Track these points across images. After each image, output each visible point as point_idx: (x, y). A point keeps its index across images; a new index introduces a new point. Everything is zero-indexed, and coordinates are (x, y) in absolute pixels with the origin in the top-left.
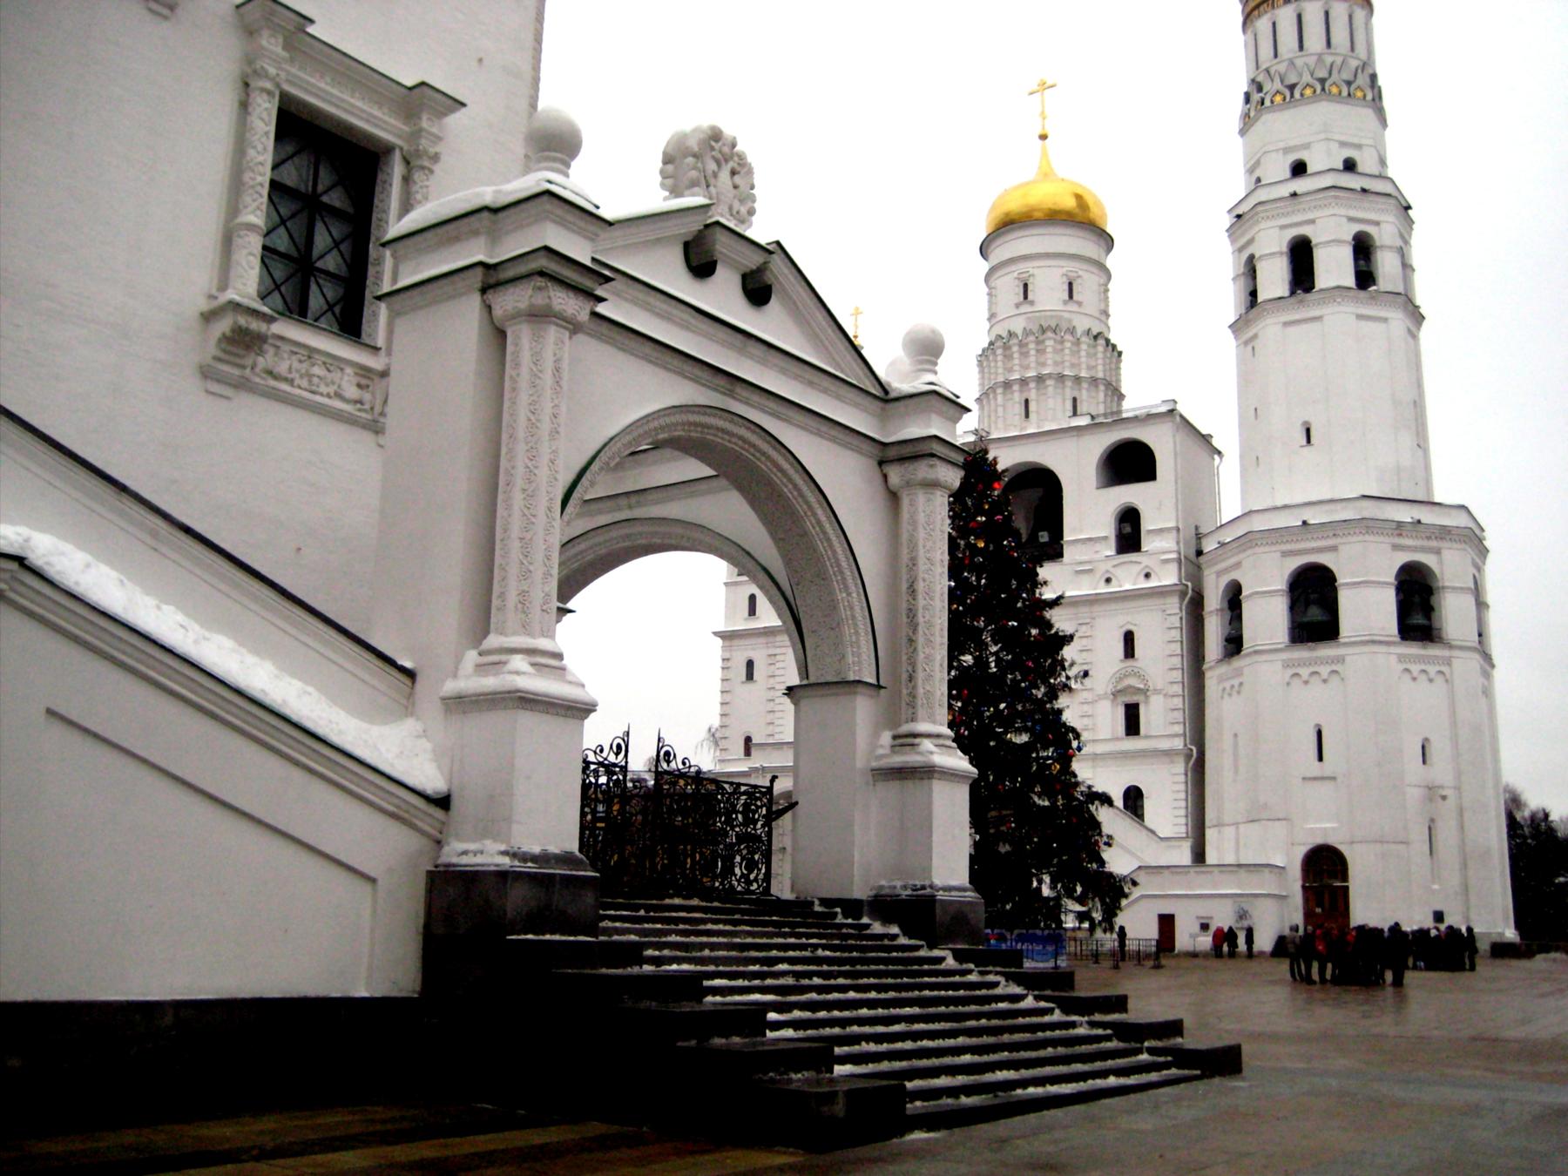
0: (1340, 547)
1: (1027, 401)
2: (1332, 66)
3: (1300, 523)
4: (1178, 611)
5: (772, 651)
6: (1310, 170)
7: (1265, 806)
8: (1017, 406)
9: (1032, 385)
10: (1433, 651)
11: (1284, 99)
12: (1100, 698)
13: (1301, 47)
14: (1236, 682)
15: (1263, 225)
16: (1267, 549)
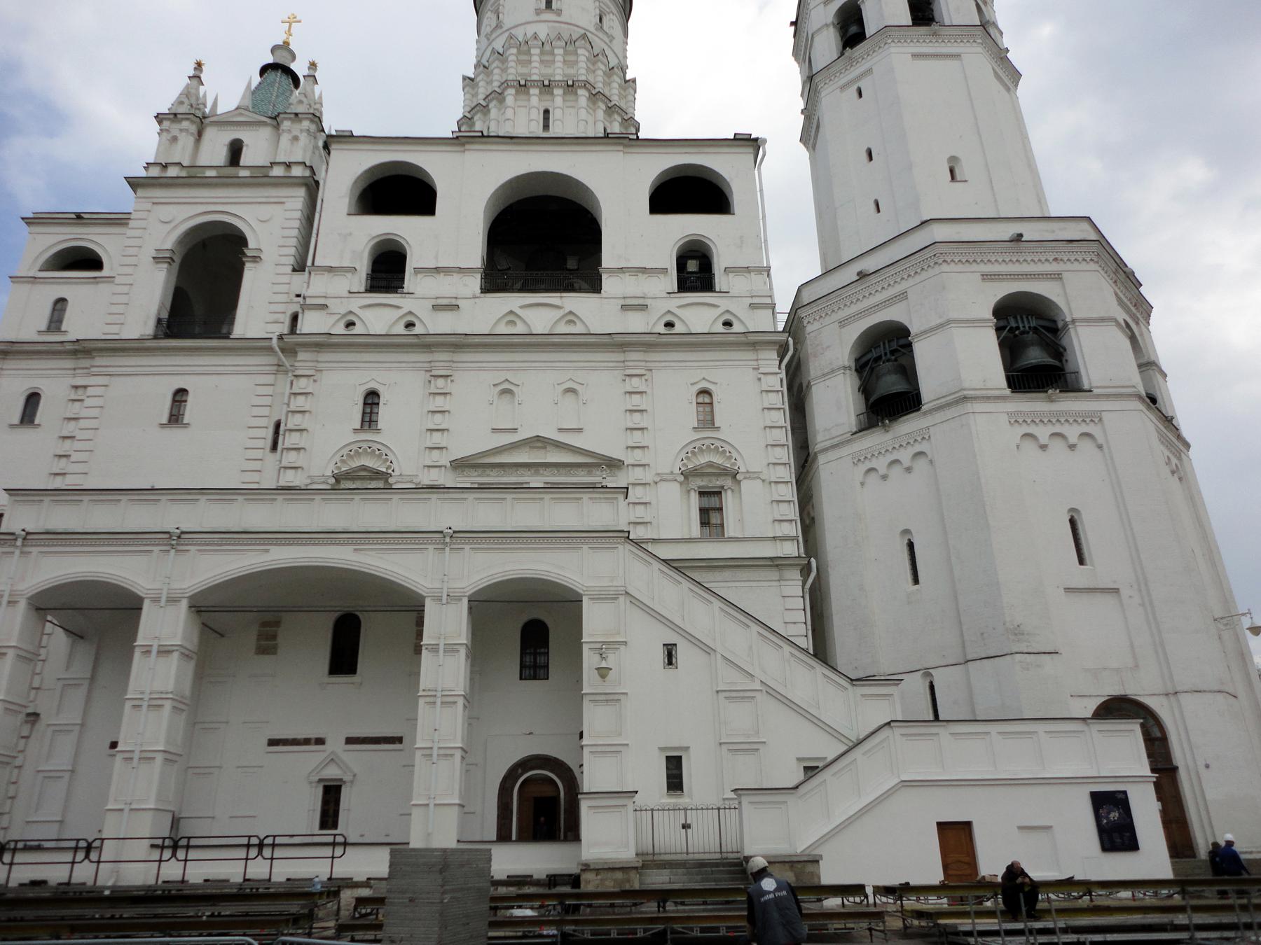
0: (1065, 275)
1: (546, 112)
4: (778, 371)
5: (80, 381)
7: (1018, 632)
8: (534, 112)
9: (558, 92)
12: (662, 479)
14: (905, 456)
16: (960, 267)
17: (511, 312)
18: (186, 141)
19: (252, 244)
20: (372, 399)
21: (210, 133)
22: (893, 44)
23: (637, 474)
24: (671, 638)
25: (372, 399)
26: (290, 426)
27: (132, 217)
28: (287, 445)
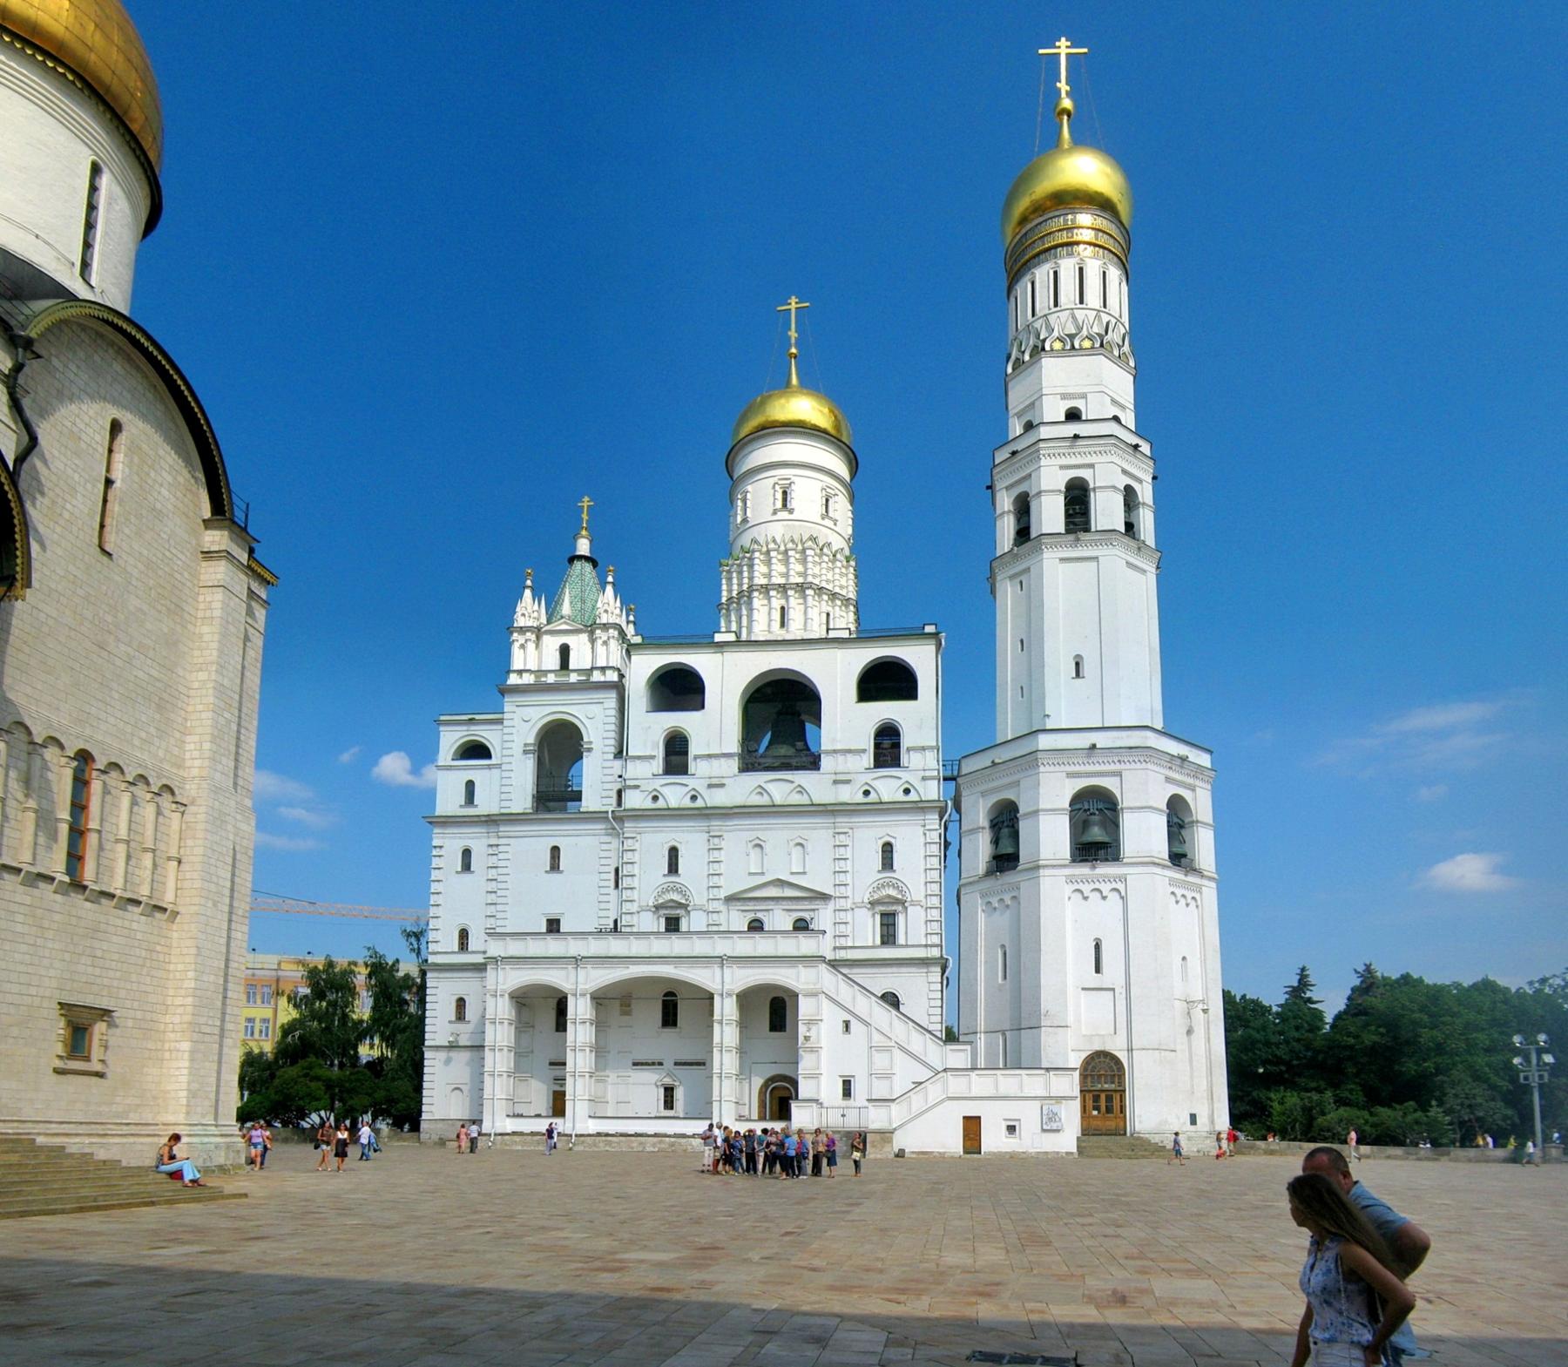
2: (1108, 324)
6: (1084, 418)
10: (1191, 879)
11: (1063, 349)
13: (1081, 302)
17: (760, 786)
18: (531, 646)
19: (585, 739)
20: (673, 853)
21: (546, 639)
23: (842, 903)
24: (848, 1017)
25: (673, 853)
26: (625, 873)
27: (506, 716)
28: (624, 886)
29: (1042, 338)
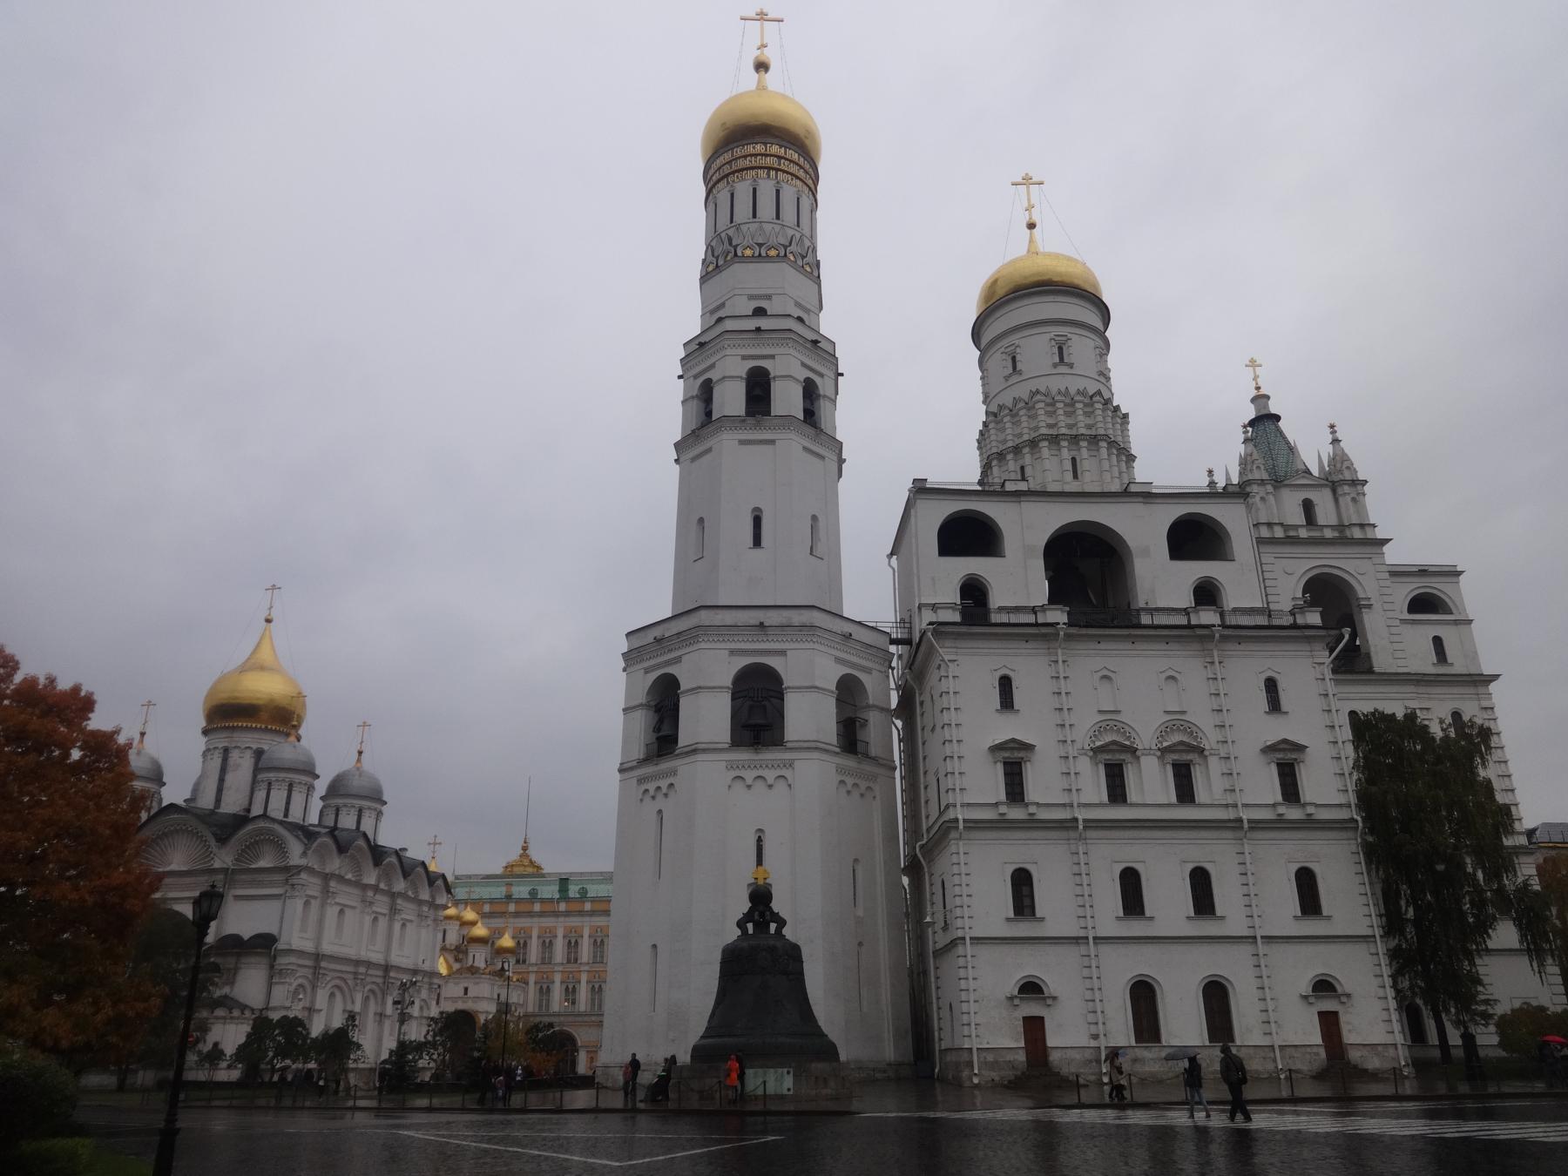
3: (758, 623)
11: (753, 256)
14: (664, 784)
15: (728, 352)
22: (726, 432)
29: (734, 244)
